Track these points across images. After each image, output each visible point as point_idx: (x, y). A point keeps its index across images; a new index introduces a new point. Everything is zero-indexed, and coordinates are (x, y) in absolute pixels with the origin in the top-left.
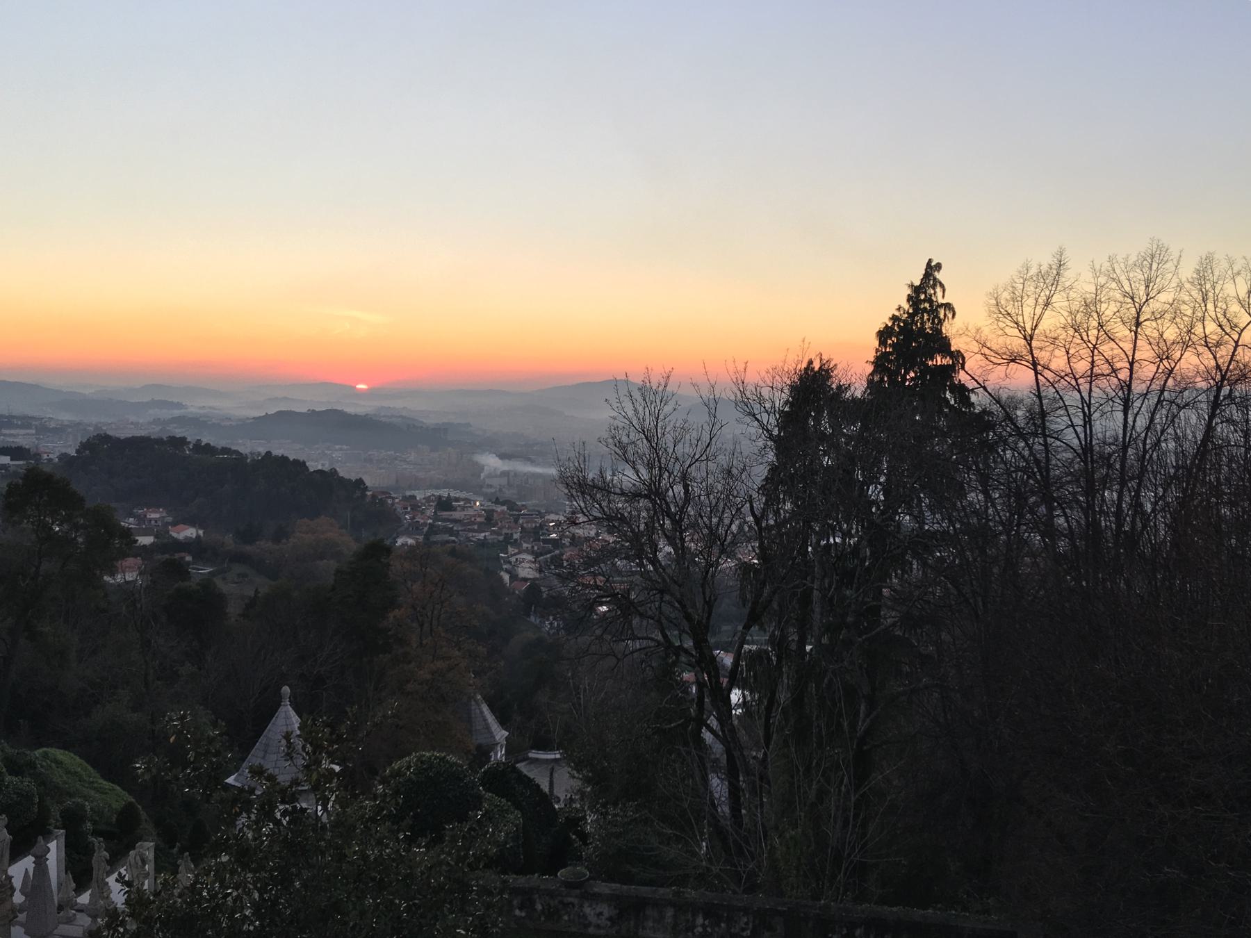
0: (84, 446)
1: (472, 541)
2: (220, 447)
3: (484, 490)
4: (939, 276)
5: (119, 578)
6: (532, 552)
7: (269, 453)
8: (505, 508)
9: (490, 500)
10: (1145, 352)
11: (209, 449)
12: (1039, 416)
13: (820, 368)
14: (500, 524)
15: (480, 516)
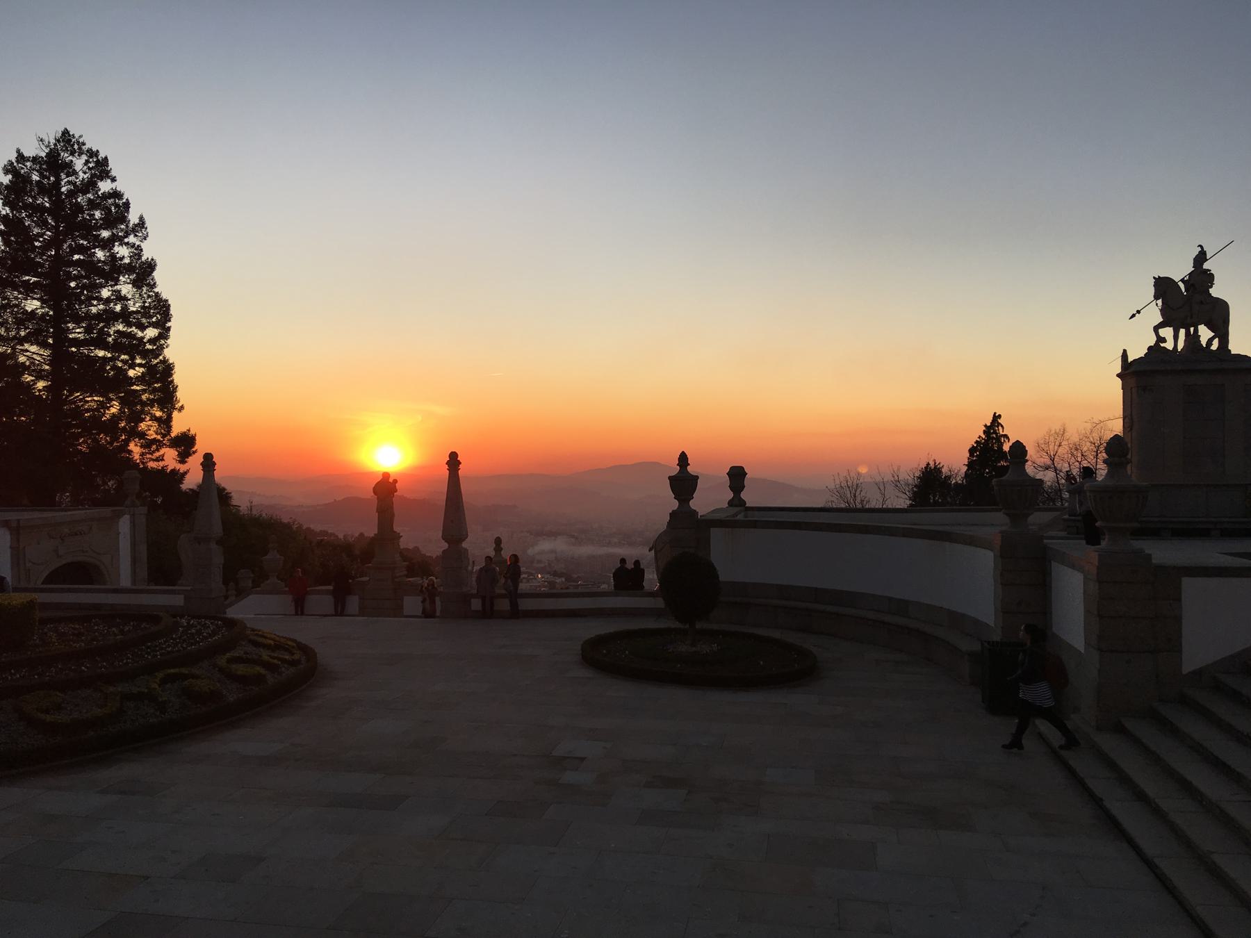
7: (362, 535)
9: (549, 573)
15: (545, 587)
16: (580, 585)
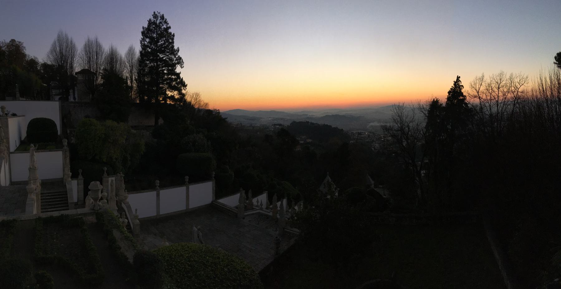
0: (292, 124)
4: (460, 79)
5: (296, 150)
7: (324, 124)
10: (501, 94)
12: (481, 108)
13: (436, 100)
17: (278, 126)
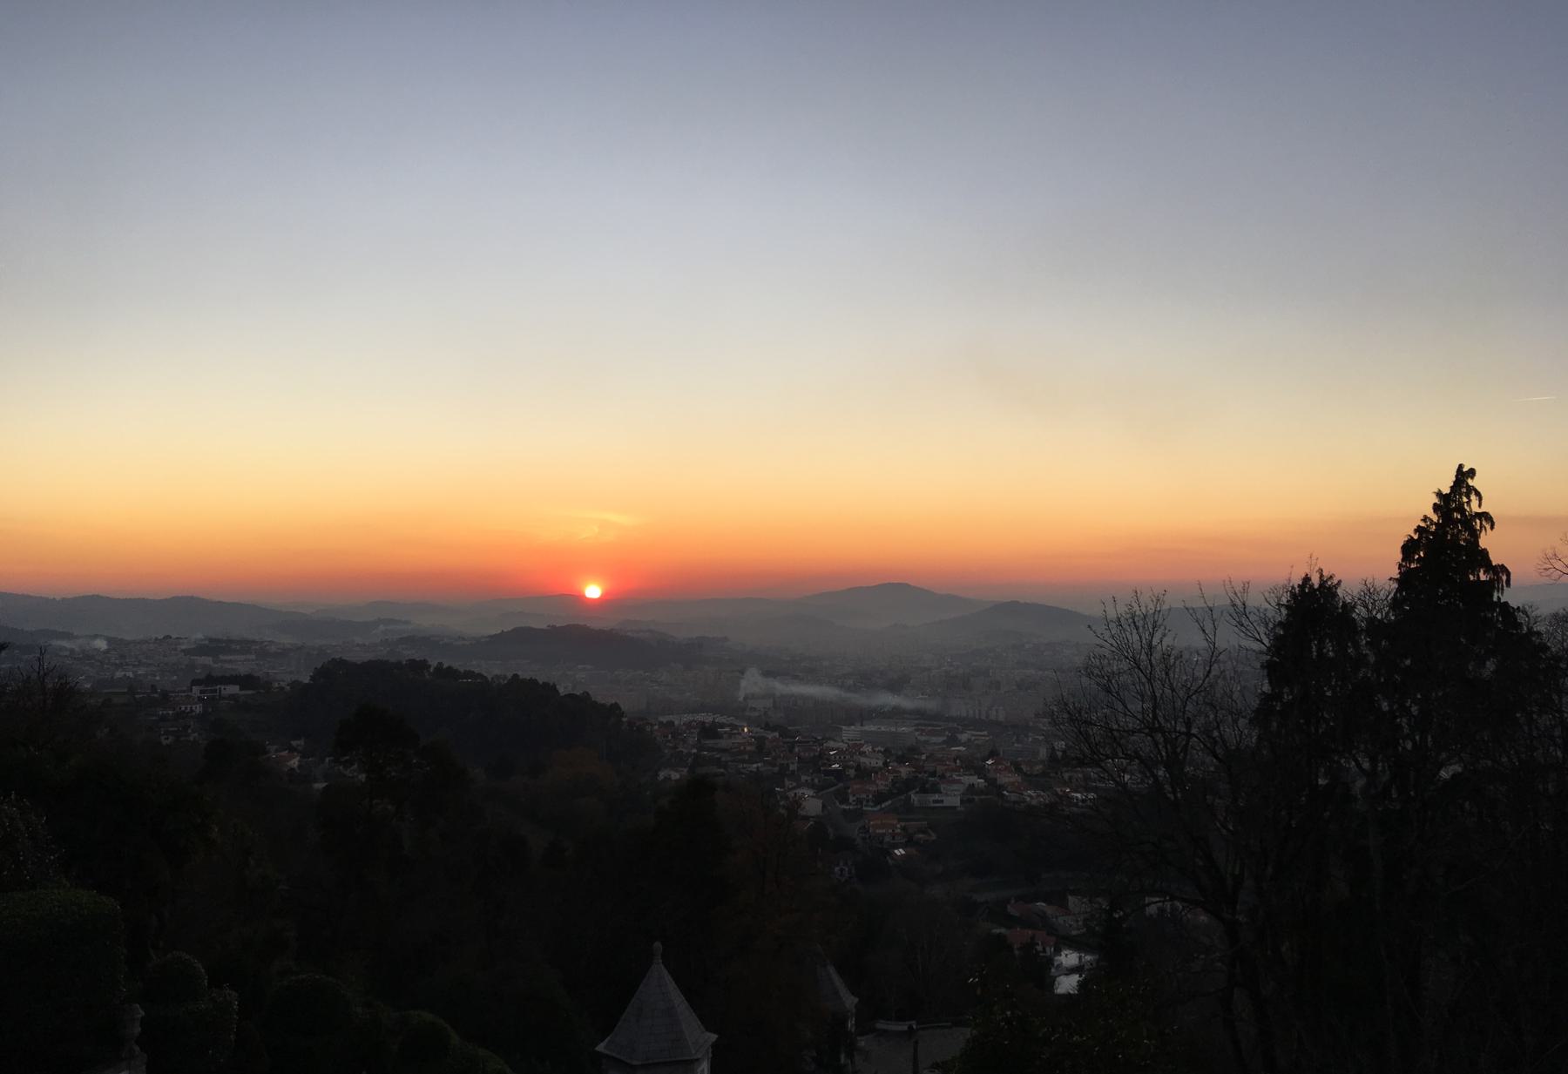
1: (743, 774)
2: (462, 670)
3: (747, 714)
6: (812, 786)
8: (777, 734)
11: (451, 673)
14: (774, 754)
15: (750, 744)
16: (801, 742)
17: (233, 689)
